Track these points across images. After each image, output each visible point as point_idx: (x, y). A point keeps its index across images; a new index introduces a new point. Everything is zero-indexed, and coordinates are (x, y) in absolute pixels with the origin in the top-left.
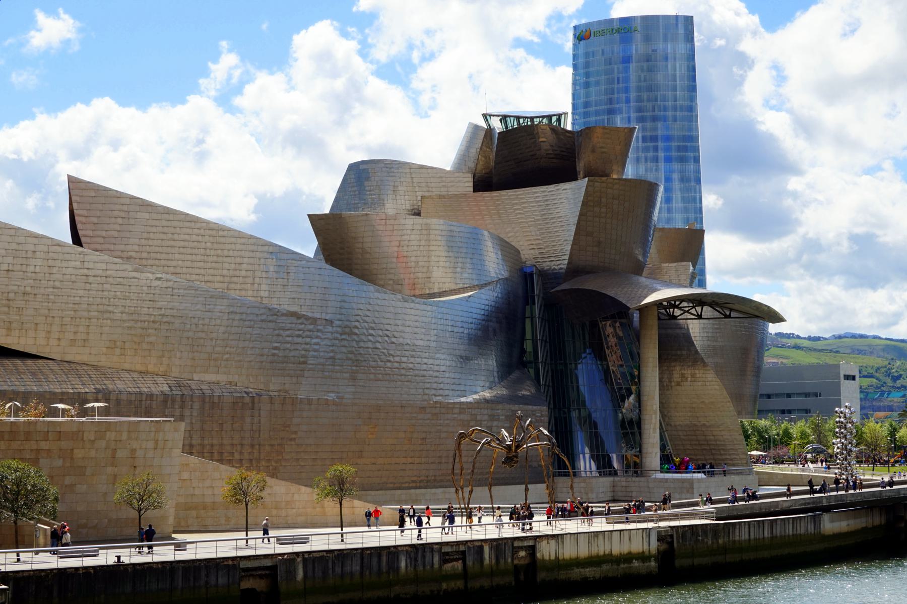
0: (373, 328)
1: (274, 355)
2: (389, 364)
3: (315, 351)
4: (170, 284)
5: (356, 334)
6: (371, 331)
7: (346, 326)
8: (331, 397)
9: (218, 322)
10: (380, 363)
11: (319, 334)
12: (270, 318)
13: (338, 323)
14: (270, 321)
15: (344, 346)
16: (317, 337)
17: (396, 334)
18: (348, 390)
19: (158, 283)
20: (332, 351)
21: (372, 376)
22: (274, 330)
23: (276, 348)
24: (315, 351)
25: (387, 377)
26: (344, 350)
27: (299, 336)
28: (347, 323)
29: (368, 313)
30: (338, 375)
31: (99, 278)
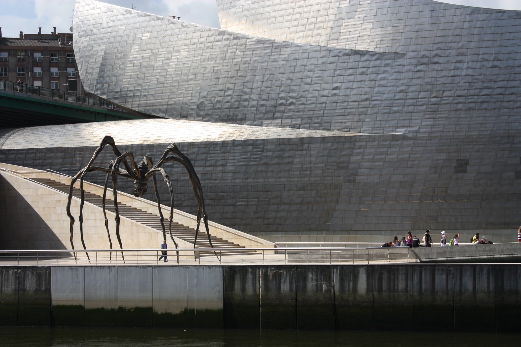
0: (462, 54)
1: (334, 95)
2: (486, 91)
3: (380, 86)
4: (243, 41)
5: (437, 63)
6: (460, 58)
7: (423, 57)
8: (400, 132)
9: (282, 70)
10: (472, 92)
11: (387, 68)
12: (331, 59)
13: (412, 54)
14: (331, 63)
15: (419, 78)
16: (385, 72)
17: (501, 56)
18: (424, 123)
19: (235, 41)
20: (403, 84)
21: (460, 106)
22: (335, 70)
23: (336, 88)
24: (380, 86)
25: (485, 105)
26: (419, 81)
27: (362, 73)
28: (425, 53)
29: (457, 38)
30: (411, 108)
31: (195, 46)
